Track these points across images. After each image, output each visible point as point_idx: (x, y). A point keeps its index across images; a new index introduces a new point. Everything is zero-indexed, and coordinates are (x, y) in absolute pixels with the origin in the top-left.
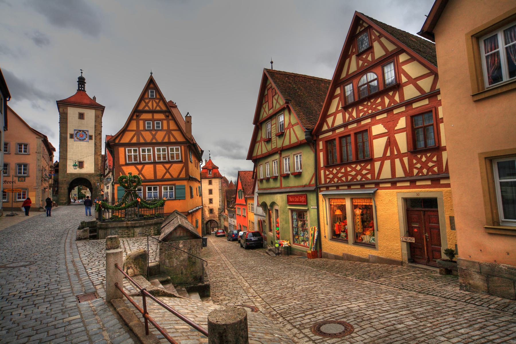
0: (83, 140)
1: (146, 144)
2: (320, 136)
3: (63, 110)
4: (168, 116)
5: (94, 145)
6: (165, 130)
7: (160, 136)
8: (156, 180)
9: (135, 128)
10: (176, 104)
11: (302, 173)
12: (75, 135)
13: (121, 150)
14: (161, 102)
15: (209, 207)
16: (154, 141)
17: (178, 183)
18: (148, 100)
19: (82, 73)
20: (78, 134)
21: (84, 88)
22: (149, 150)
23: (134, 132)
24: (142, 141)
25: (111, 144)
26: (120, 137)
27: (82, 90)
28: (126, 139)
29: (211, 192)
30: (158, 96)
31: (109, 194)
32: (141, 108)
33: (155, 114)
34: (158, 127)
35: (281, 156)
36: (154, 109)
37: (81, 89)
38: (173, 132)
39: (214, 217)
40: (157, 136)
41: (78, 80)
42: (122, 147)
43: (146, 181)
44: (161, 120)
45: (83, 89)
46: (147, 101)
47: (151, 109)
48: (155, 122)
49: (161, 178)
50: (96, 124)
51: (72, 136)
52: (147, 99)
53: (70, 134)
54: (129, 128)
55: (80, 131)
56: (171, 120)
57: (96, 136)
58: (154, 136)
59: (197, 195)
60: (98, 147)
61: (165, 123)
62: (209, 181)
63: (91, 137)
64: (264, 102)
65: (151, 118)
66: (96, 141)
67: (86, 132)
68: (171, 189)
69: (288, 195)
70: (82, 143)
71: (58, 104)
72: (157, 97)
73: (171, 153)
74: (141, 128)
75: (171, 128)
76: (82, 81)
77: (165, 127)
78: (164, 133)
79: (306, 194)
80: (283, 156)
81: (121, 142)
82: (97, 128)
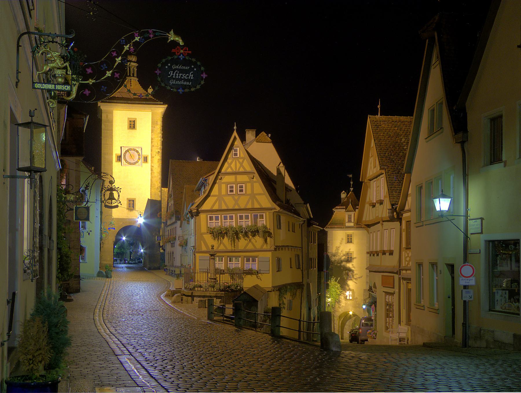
0: (134, 164)
2: (404, 215)
4: (253, 178)
5: (150, 172)
6: (248, 195)
7: (243, 202)
16: (237, 207)
17: (261, 254)
24: (224, 207)
25: (193, 211)
33: (238, 176)
35: (382, 228)
36: (237, 170)
38: (257, 196)
46: (229, 161)
47: (234, 170)
50: (154, 137)
51: (119, 158)
53: (116, 154)
55: (131, 149)
56: (255, 182)
57: (153, 156)
61: (249, 185)
63: (146, 160)
72: (241, 156)
77: (249, 191)
80: (384, 228)
82: (153, 143)
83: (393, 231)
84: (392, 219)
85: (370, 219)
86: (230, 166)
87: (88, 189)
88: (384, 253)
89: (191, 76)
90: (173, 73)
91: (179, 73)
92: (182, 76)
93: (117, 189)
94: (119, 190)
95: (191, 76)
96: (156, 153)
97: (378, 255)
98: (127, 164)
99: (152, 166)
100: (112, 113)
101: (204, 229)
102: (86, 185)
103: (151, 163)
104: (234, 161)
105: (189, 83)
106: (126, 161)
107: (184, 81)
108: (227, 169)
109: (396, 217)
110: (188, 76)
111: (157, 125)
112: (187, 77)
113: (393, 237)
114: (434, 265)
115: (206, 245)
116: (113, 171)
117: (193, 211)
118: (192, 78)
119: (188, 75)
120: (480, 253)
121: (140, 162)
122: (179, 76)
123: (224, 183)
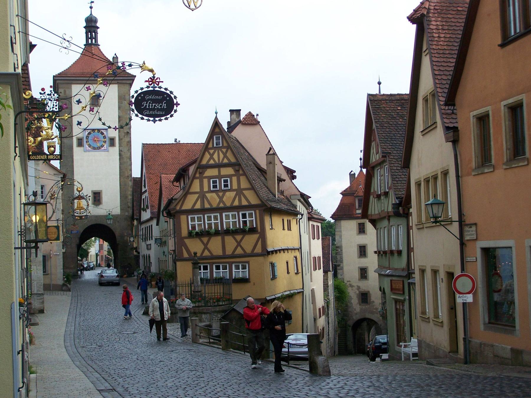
0: (99, 148)
1: (212, 210)
3: (65, 92)
4: (238, 171)
5: (118, 157)
7: (229, 197)
8: (224, 257)
9: (198, 189)
10: (259, 119)
11: (402, 252)
12: (85, 140)
13: (183, 218)
14: (229, 151)
15: (359, 287)
16: (221, 205)
18: (213, 151)
19: (91, 8)
20: (90, 136)
21: (96, 38)
22: (216, 218)
23: (197, 196)
24: (207, 206)
26: (181, 202)
27: (94, 45)
28: (188, 205)
29: (362, 251)
30: (225, 144)
31: (153, 260)
32: (204, 162)
34: (226, 186)
36: (220, 162)
37: (92, 41)
39: (372, 313)
40: (224, 199)
41: (84, 24)
42: (184, 215)
43: (213, 257)
44: (230, 176)
45: (94, 40)
47: (217, 162)
48: (222, 180)
49: (230, 253)
50: (121, 114)
51: (80, 143)
52: (211, 149)
54: (191, 190)
55: (93, 130)
56: (242, 175)
57: (121, 137)
58: (221, 198)
59: (288, 273)
60: (125, 160)
61: (235, 179)
62: (359, 224)
63: (112, 142)
64: (372, 140)
65: (217, 174)
66: (121, 149)
67: (103, 131)
68: (244, 268)
69: (391, 281)
70: (97, 153)
71: (55, 81)
72: (224, 145)
73: (242, 221)
74: (206, 189)
75: (242, 187)
76: (93, 24)
77: (235, 186)
78: (233, 194)
79: (403, 281)
80: (391, 224)
81: (184, 208)
82: (121, 122)
83: (401, 227)
84: (397, 214)
85: (376, 213)
86: (212, 157)
87: (54, 199)
88: (392, 252)
89: (164, 106)
90: (146, 103)
91: (152, 103)
92: (155, 106)
93: (85, 197)
94: (88, 198)
95: (164, 106)
96: (124, 134)
97: (386, 256)
98: (90, 149)
99: (120, 151)
100: (71, 89)
101: (184, 232)
102: (52, 194)
103: (119, 146)
104: (217, 151)
105: (163, 113)
106: (90, 146)
107: (157, 111)
108: (209, 160)
109: (401, 212)
110: (161, 106)
111: (125, 100)
112: (160, 107)
113: (401, 234)
114: (435, 272)
115: (188, 251)
116: (74, 158)
117: (172, 212)
118: (165, 107)
119: (161, 104)
120: (476, 261)
121: (105, 146)
122: (152, 106)
123: (206, 177)
